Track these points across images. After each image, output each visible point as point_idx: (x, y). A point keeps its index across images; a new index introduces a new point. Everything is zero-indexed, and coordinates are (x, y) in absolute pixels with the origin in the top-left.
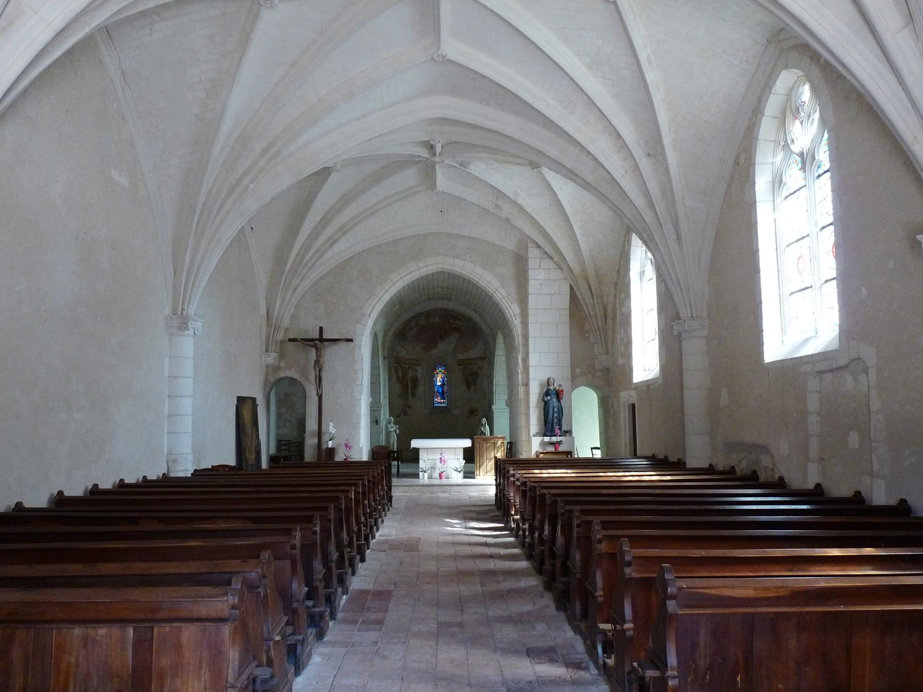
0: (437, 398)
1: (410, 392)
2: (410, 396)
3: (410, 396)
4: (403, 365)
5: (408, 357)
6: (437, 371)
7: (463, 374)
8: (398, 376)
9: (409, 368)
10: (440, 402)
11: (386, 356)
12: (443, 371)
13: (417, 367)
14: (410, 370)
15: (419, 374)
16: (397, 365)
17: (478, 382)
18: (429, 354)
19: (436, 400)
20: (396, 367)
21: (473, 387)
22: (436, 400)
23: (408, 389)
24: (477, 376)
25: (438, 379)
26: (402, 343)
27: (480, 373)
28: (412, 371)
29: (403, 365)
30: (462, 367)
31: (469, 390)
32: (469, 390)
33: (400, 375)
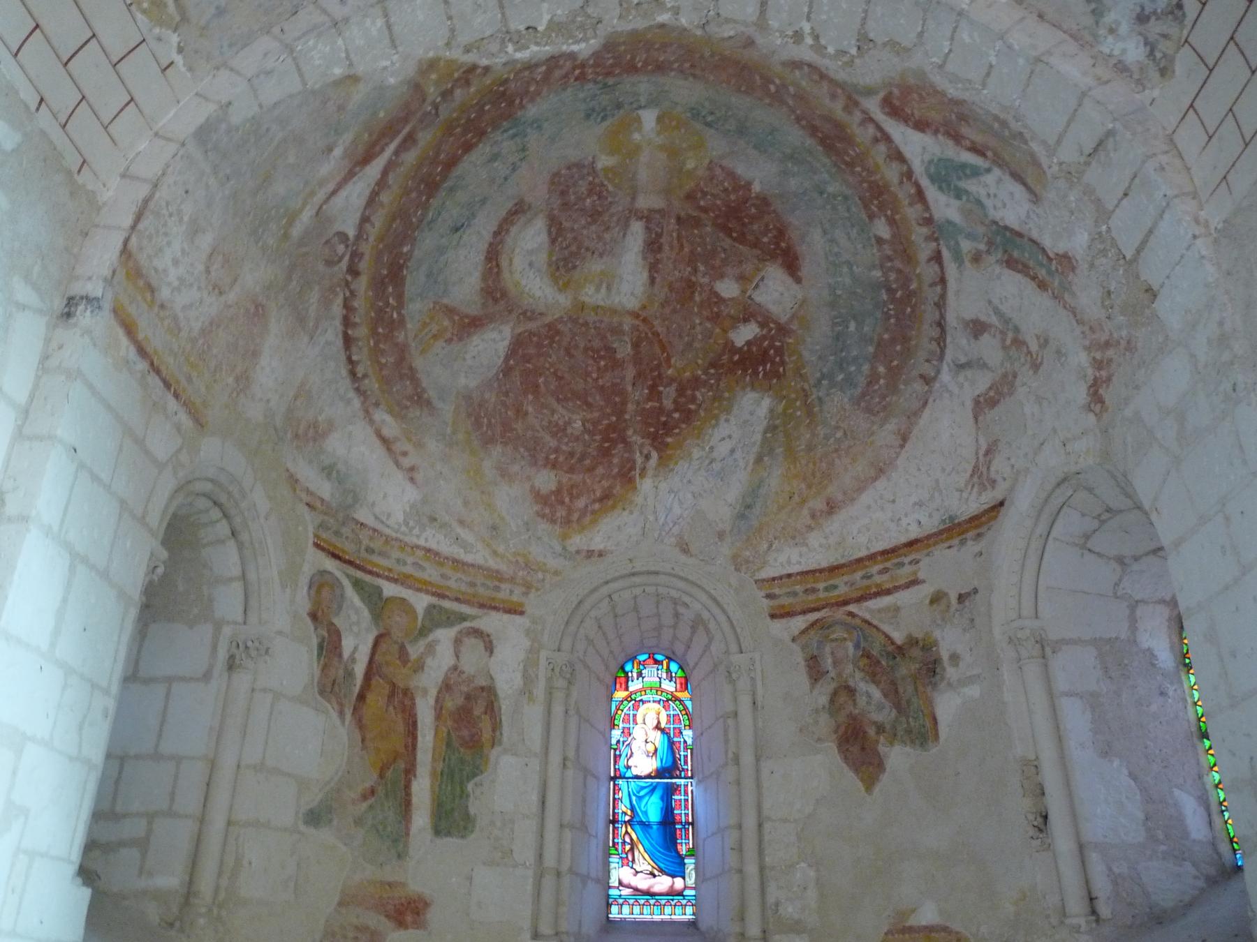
0: (628, 861)
1: (422, 788)
2: (421, 819)
3: (421, 819)
4: (389, 589)
5: (433, 539)
6: (634, 685)
7: (815, 670)
8: (330, 647)
9: (437, 618)
10: (648, 893)
11: (95, 288)
12: (669, 686)
13: (491, 622)
14: (444, 636)
15: (507, 679)
16: (330, 565)
17: (947, 706)
18: (577, 541)
19: (625, 874)
20: (321, 584)
21: (897, 757)
22: (625, 874)
23: (410, 771)
24: (932, 669)
25: (638, 732)
26: (391, 427)
27: (949, 640)
28: (458, 642)
29: (389, 589)
30: (799, 623)
31: (870, 783)
32: (870, 783)
33: (347, 644)
